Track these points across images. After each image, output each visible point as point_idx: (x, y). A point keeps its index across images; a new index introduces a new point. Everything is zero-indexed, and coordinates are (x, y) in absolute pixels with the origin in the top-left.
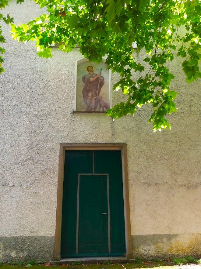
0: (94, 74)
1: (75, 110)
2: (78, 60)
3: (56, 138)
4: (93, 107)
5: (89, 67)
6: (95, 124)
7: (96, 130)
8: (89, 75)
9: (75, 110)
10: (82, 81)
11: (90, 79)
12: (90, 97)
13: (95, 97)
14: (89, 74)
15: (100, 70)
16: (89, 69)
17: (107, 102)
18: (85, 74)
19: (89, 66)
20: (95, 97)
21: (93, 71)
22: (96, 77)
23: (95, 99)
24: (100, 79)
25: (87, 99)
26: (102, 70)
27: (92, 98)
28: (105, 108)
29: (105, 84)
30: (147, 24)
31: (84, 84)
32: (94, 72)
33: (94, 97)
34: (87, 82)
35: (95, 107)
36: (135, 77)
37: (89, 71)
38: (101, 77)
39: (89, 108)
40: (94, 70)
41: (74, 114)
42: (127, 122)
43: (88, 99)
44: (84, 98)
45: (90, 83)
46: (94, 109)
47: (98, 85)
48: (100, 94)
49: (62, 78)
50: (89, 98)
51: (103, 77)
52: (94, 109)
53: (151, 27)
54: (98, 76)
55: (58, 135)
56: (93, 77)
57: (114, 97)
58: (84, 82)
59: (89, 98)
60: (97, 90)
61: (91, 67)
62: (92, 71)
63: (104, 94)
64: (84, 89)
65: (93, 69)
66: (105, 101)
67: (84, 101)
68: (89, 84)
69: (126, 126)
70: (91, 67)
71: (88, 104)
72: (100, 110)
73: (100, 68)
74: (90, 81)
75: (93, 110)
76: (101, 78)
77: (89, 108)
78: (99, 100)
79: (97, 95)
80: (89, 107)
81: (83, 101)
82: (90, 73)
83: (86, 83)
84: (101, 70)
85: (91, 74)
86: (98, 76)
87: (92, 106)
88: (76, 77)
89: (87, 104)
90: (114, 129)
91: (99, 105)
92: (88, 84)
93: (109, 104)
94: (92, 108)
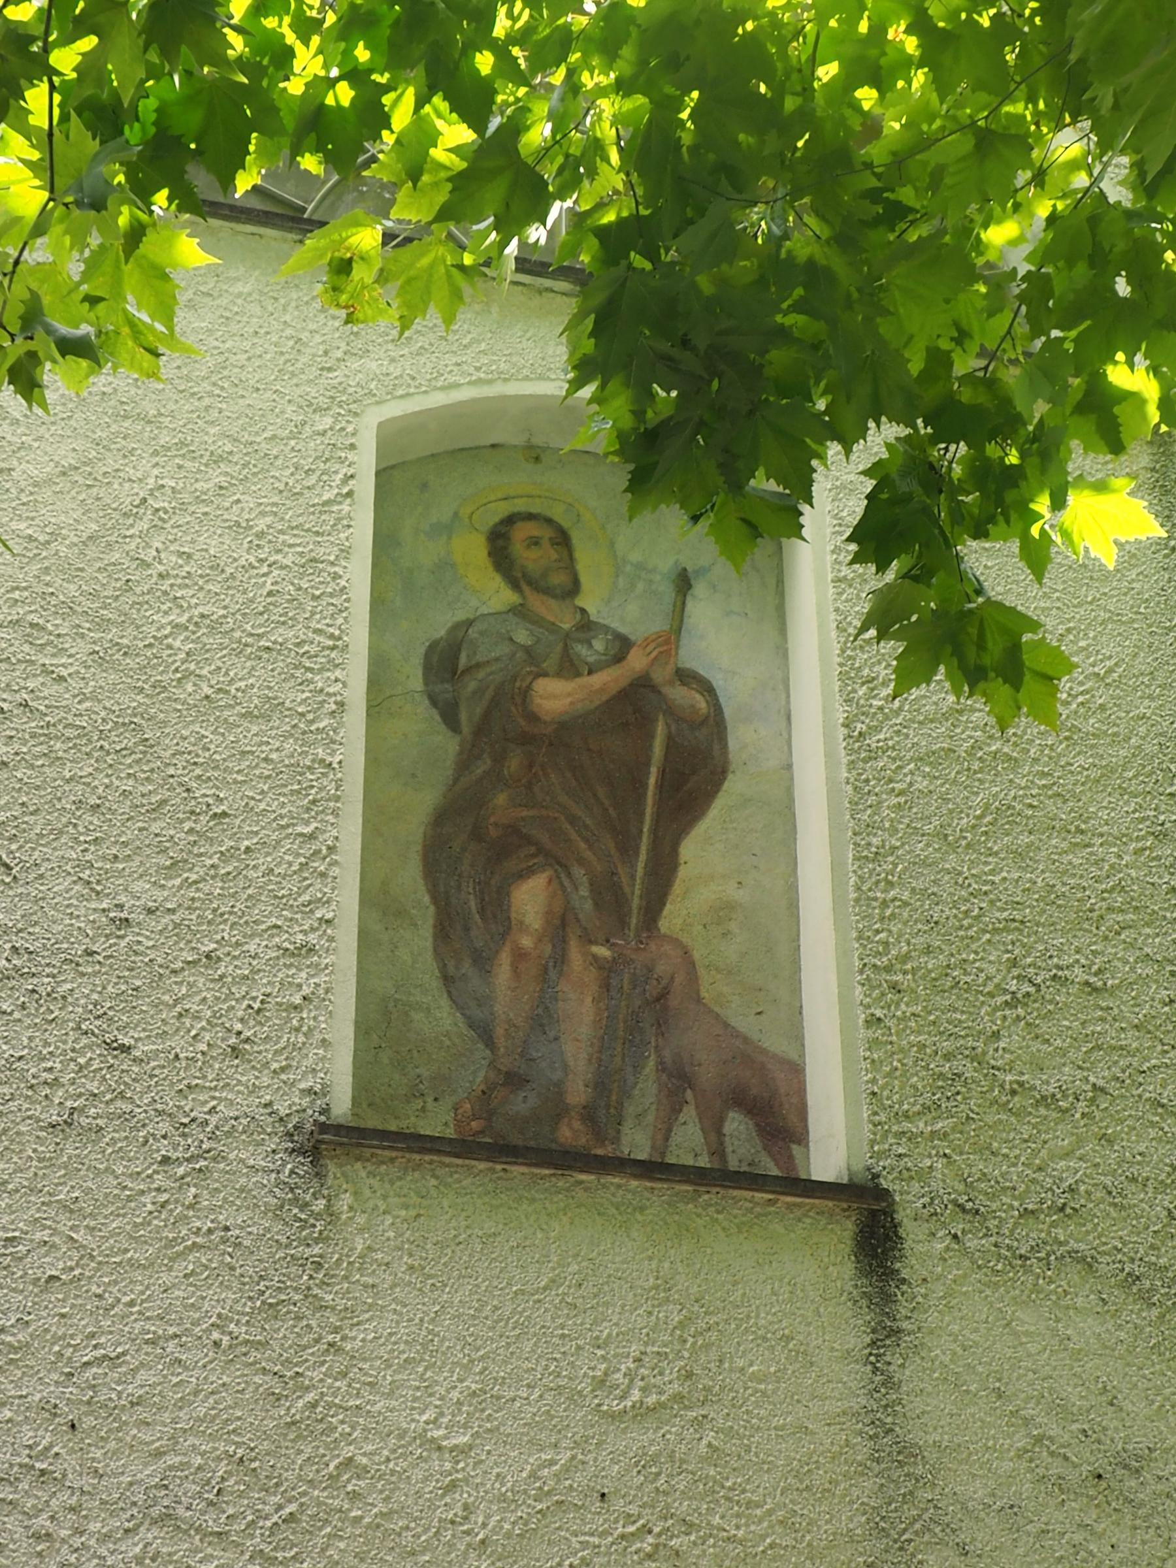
0: (586, 626)
1: (342, 1105)
2: (394, 409)
3: (42, 1522)
4: (578, 1093)
5: (522, 532)
6: (635, 1349)
7: (643, 1438)
8: (522, 636)
9: (342, 1105)
10: (423, 707)
11: (526, 692)
12: (526, 942)
13: (603, 951)
14: (519, 612)
15: (667, 591)
16: (530, 558)
17: (775, 1043)
18: (461, 615)
19: (520, 506)
20: (603, 951)
21: (574, 588)
22: (608, 680)
23: (607, 971)
24: (671, 711)
25: (483, 962)
26: (700, 589)
27: (560, 959)
28: (736, 1124)
29: (734, 787)
30: (934, 127)
31: (449, 745)
32: (591, 601)
33: (588, 939)
34: (487, 715)
35: (601, 1084)
36: (1150, 748)
37: (515, 585)
38: (686, 677)
39: (522, 1104)
40: (583, 579)
41: (332, 1168)
42: (1077, 1355)
43: (505, 959)
44: (442, 932)
45: (525, 739)
46: (589, 1114)
47: (639, 785)
48: (671, 919)
49: (162, 618)
50: (520, 955)
51: (708, 689)
52: (589, 1114)
53: (1074, 166)
54: (637, 661)
55: (70, 1463)
56: (569, 667)
57: (895, 987)
58: (449, 715)
59: (520, 955)
60: (628, 849)
61: (546, 533)
62: (558, 579)
63: (723, 911)
64: (440, 818)
65: (578, 555)
66: (744, 1022)
67: (447, 980)
68: (514, 763)
69: (1063, 1411)
70: (546, 533)
71: (499, 1031)
72: (677, 1136)
73: (665, 565)
74: (533, 718)
75: (571, 1133)
76: (680, 695)
77: (522, 1104)
78: (663, 996)
79: (623, 923)
80: (514, 1080)
81: (434, 983)
82: (539, 605)
83: (480, 731)
84: (684, 582)
85: (553, 628)
86: (637, 661)
87: (557, 1075)
88: (359, 637)
89: (485, 1034)
90: (907, 1453)
91: (662, 1067)
92: (500, 759)
93: (797, 1070)
94: (557, 1109)
